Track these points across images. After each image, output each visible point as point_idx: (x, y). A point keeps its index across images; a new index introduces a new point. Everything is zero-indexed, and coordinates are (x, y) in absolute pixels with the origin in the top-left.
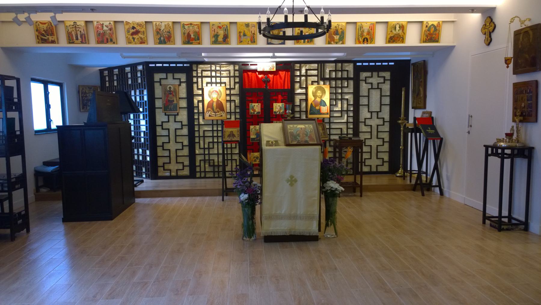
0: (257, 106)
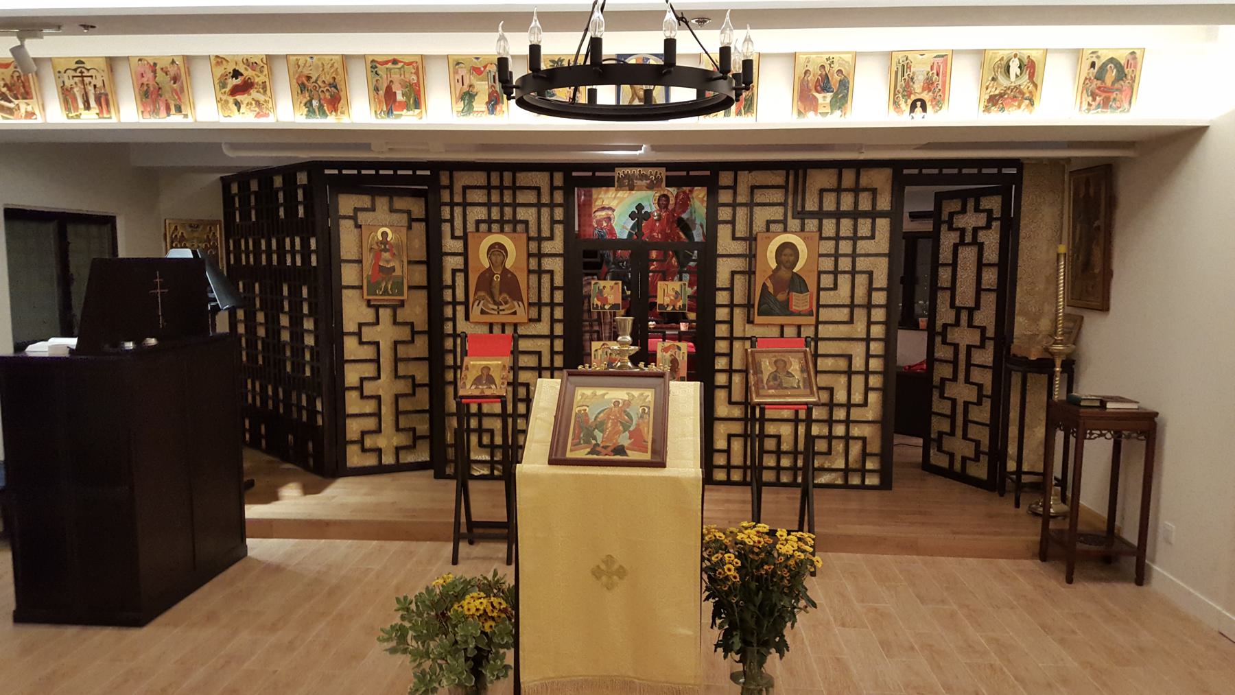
0: (612, 288)
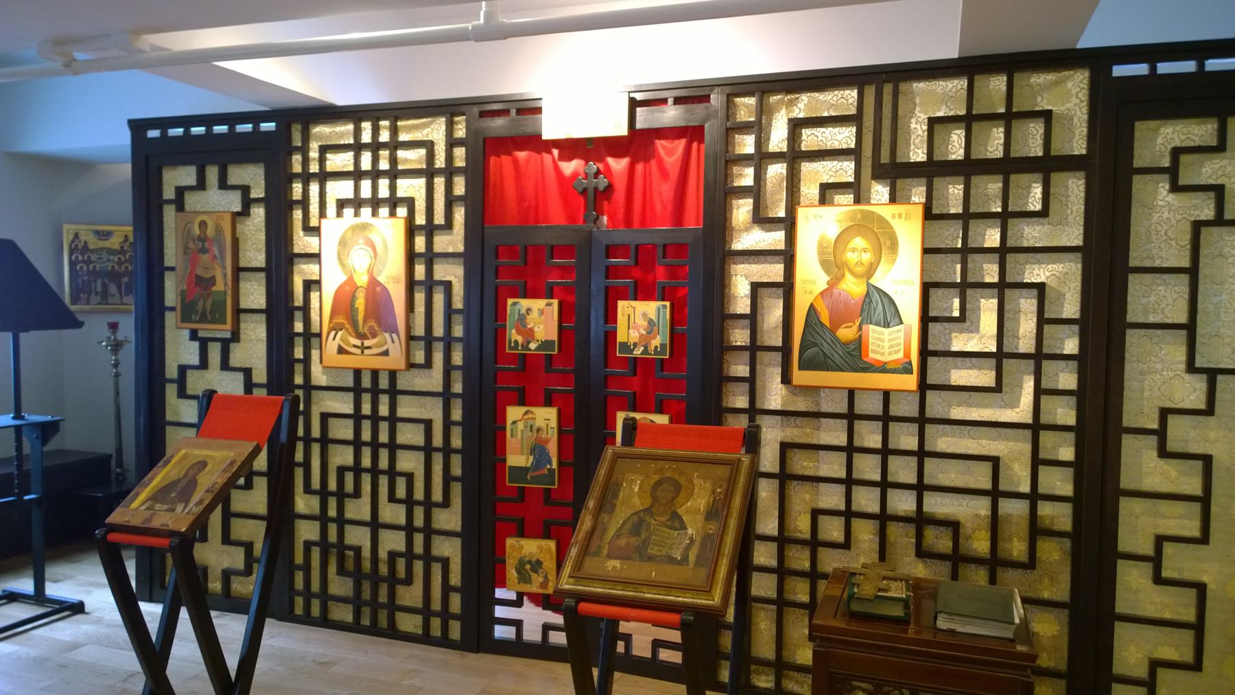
0: (542, 312)
